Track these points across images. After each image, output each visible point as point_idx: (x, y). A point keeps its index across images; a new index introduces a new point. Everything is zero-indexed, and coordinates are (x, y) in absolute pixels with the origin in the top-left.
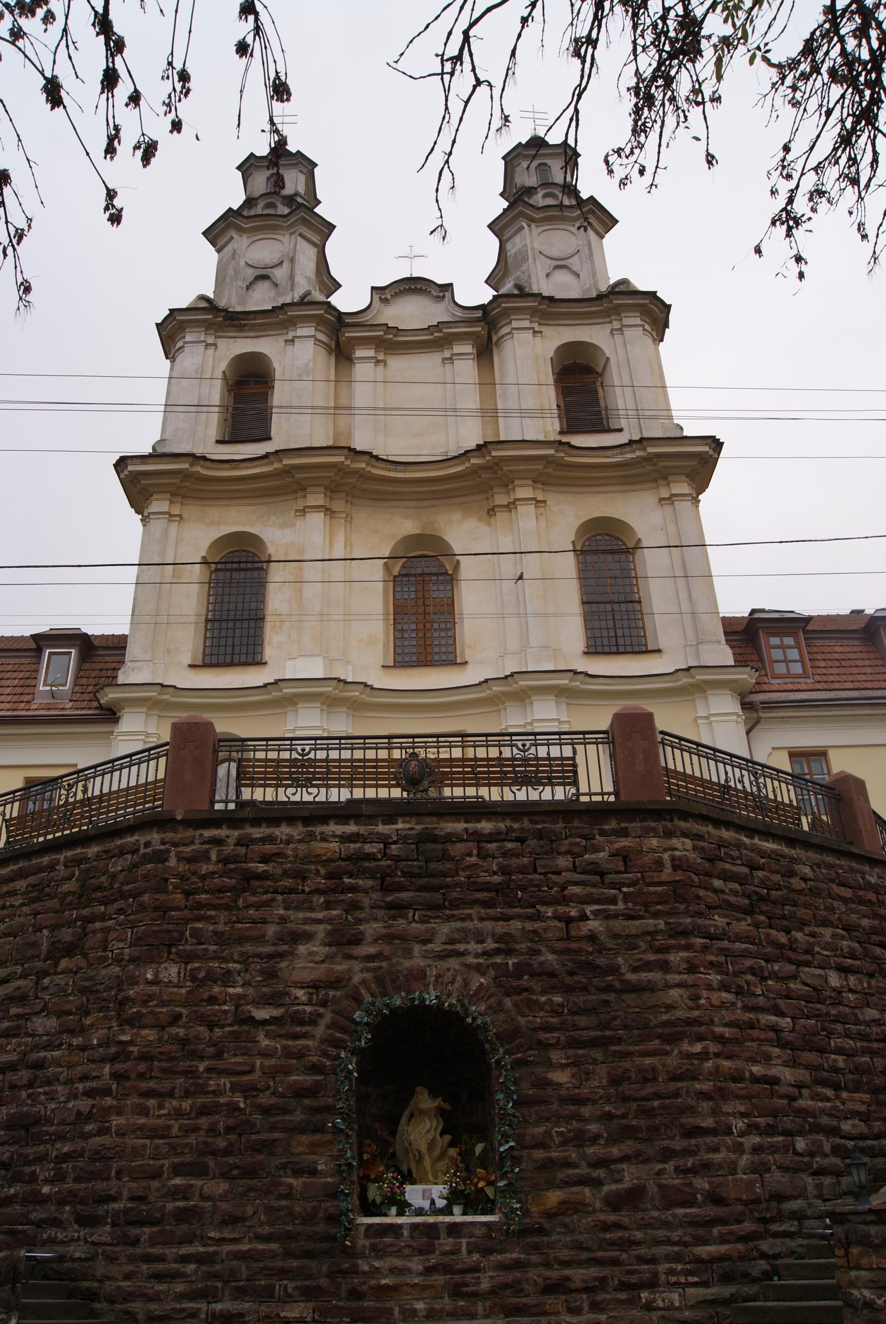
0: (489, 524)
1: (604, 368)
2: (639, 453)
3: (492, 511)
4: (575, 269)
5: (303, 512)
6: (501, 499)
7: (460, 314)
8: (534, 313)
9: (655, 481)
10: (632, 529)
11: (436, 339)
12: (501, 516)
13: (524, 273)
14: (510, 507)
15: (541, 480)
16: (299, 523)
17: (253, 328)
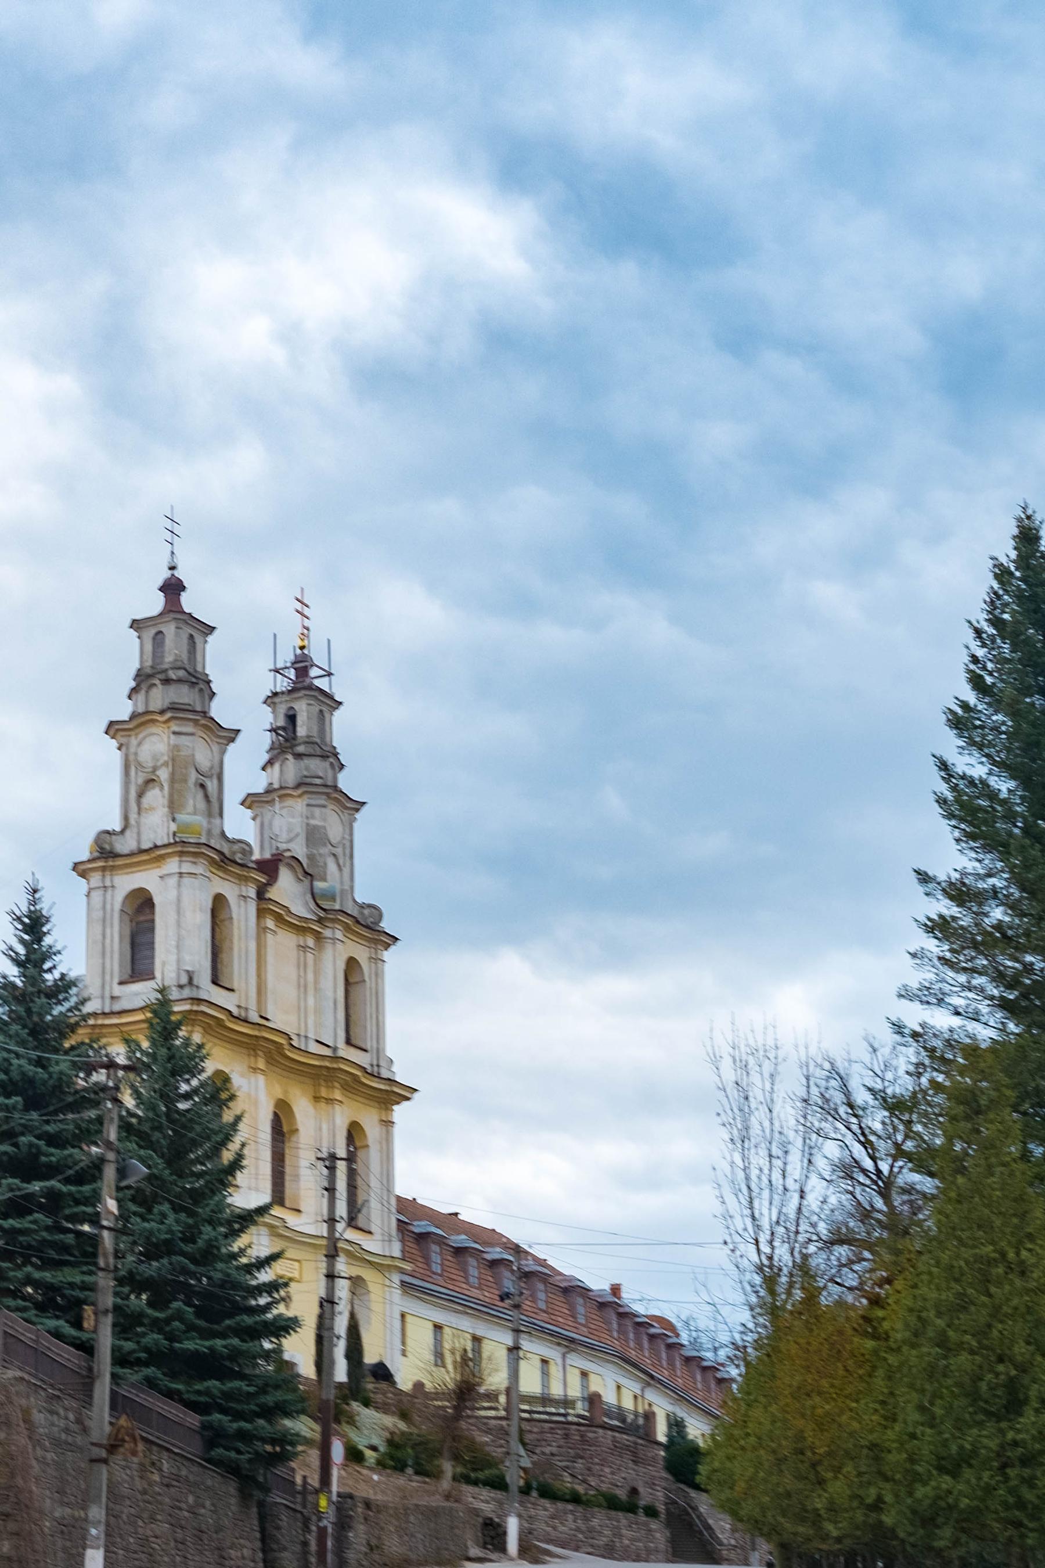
0: (315, 1108)
1: (357, 983)
2: (387, 1088)
3: (317, 1099)
4: (341, 862)
5: (255, 1070)
6: (324, 1092)
7: (312, 905)
8: (347, 928)
9: (378, 1102)
10: (365, 1136)
11: (300, 929)
12: (323, 1105)
13: (320, 855)
14: (330, 1101)
15: (346, 1088)
16: (253, 1077)
17: (226, 871)
